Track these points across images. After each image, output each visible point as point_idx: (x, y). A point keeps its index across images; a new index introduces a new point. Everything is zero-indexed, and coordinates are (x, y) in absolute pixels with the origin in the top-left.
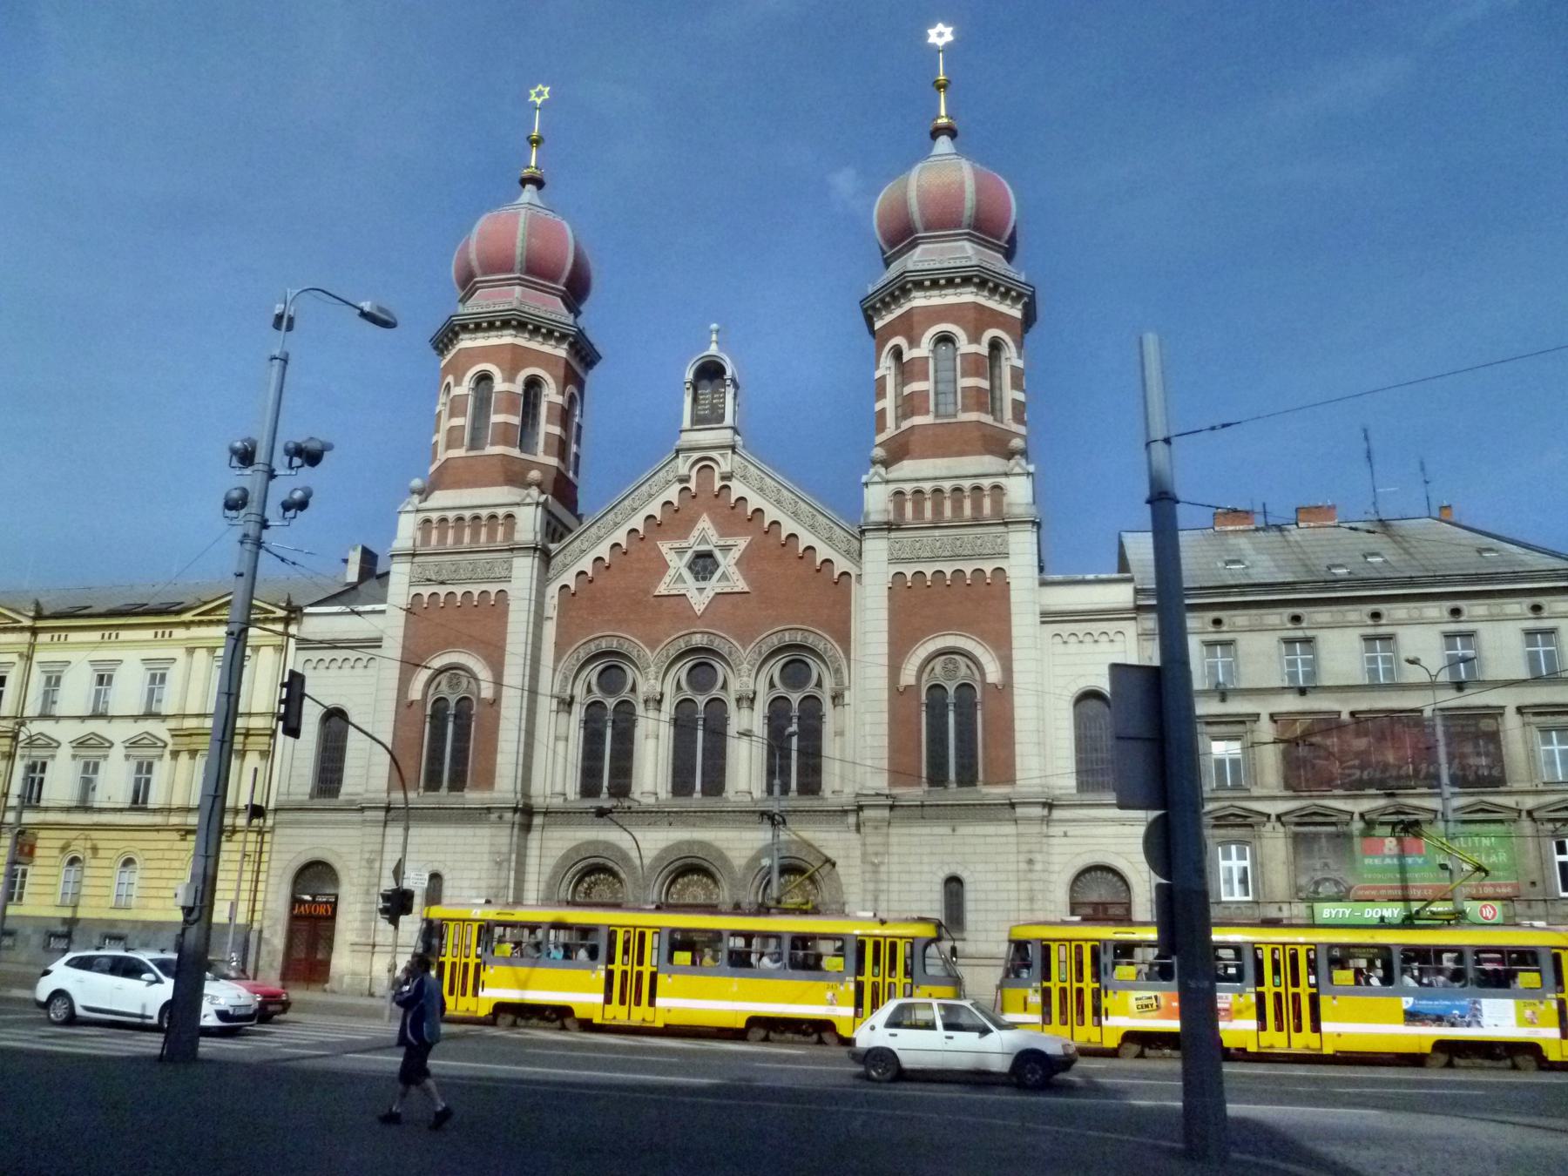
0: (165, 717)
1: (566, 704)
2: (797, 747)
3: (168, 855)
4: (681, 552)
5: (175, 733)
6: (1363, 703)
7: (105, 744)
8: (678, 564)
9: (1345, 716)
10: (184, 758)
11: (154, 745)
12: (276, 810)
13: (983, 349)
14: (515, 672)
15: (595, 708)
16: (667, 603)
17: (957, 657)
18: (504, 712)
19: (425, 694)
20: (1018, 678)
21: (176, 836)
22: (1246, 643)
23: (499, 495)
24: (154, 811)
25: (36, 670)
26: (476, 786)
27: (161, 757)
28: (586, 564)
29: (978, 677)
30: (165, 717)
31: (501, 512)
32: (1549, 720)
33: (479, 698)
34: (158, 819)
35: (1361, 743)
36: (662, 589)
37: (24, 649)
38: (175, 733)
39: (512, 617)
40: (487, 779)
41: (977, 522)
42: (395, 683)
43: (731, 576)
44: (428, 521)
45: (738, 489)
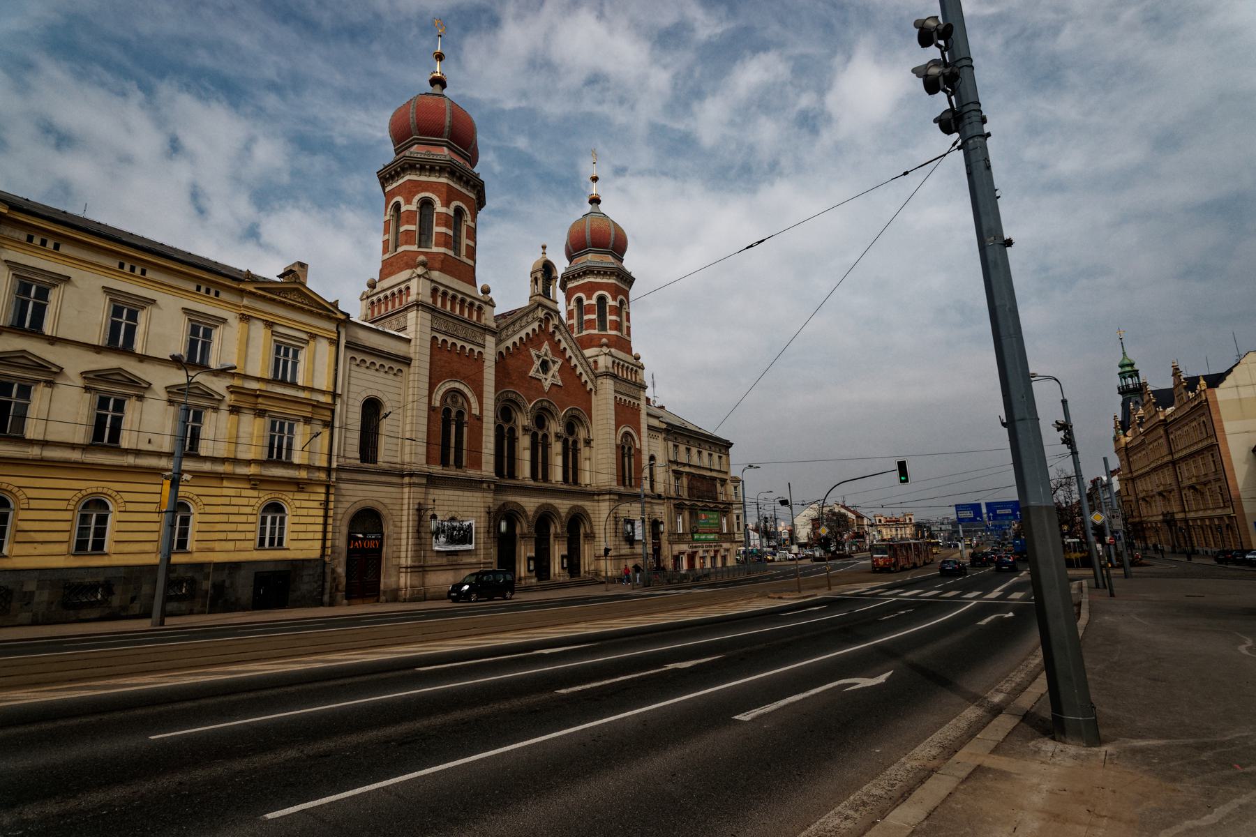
3: (235, 500)
4: (538, 357)
5: (233, 390)
8: (537, 363)
12: (339, 469)
34: (220, 468)
36: (532, 373)
40: (477, 464)
45: (558, 337)
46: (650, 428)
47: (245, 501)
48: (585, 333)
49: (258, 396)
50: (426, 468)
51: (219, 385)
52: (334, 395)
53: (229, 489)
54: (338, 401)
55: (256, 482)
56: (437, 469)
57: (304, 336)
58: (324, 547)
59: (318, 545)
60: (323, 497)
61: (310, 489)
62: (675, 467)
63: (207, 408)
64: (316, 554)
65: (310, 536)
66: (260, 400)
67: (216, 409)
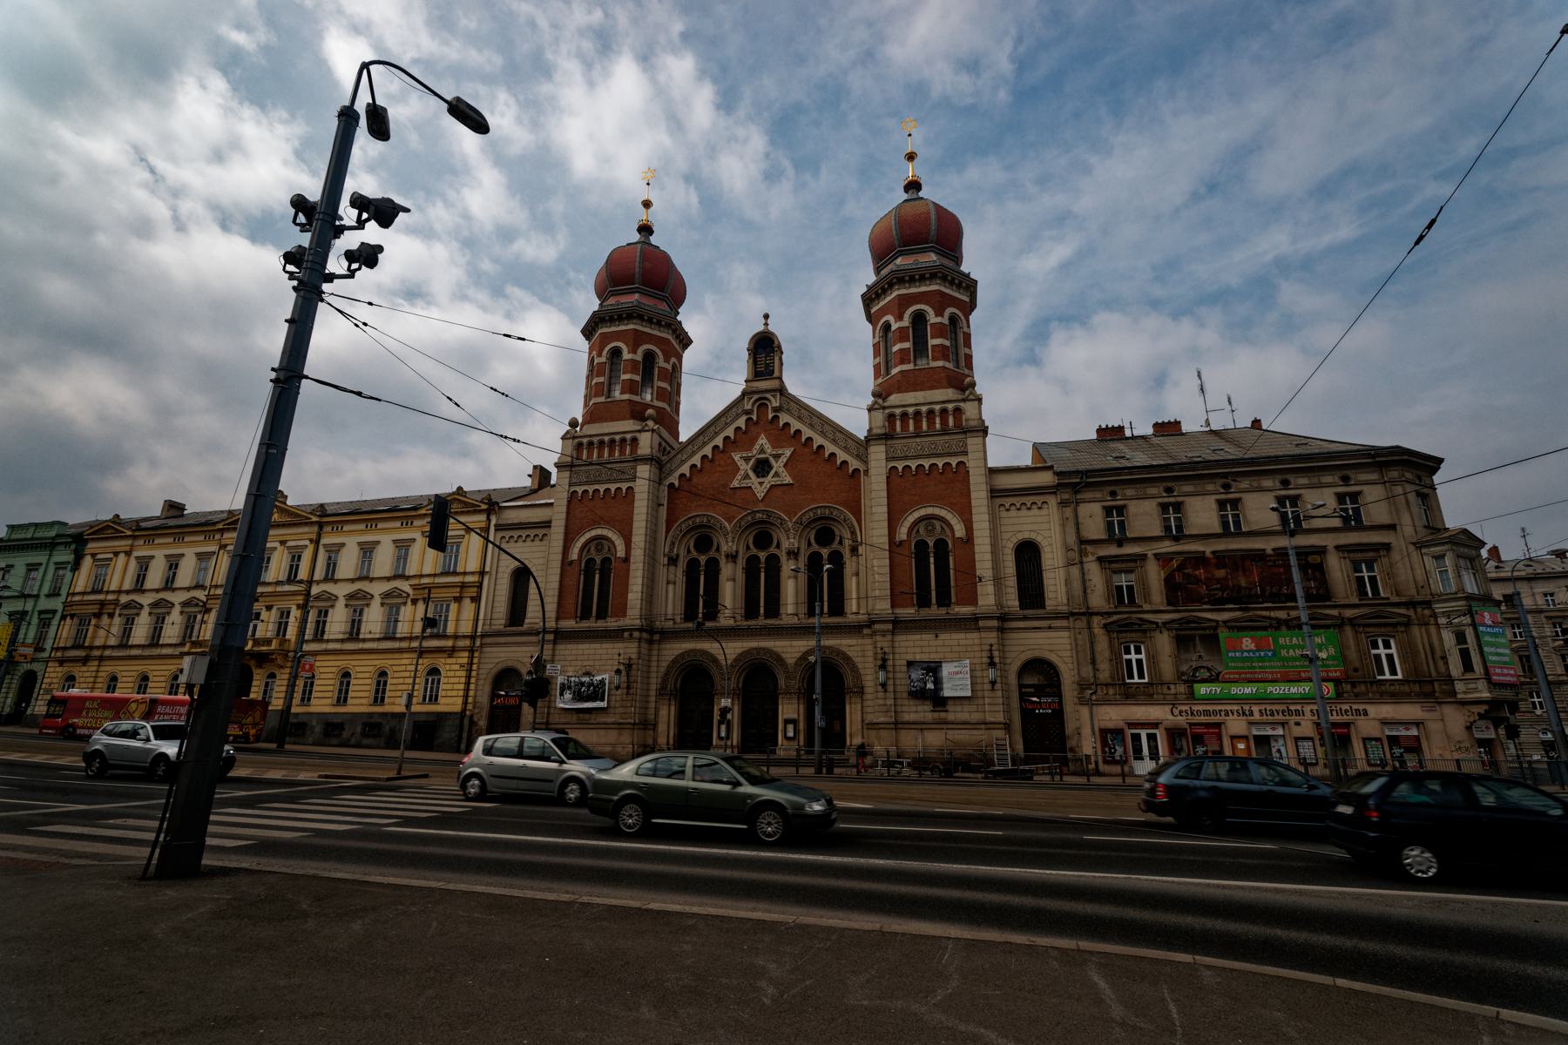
0: (408, 578)
1: (673, 561)
2: (826, 586)
4: (747, 460)
6: (1221, 545)
7: (366, 597)
8: (745, 467)
9: (1208, 554)
11: (400, 596)
12: (482, 636)
13: (945, 321)
14: (639, 538)
15: (692, 566)
18: (632, 567)
22: (1134, 508)
23: (628, 425)
24: (401, 639)
25: (321, 550)
30: (408, 578)
32: (1359, 556)
34: (404, 644)
35: (1221, 573)
36: (735, 484)
37: (314, 537)
39: (637, 504)
40: (622, 611)
41: (945, 431)
42: (560, 549)
43: (781, 473)
44: (580, 445)
45: (784, 418)
51: (405, 586)
55: (422, 652)
58: (465, 703)
59: (460, 701)
60: (465, 661)
62: (1113, 550)
64: (458, 708)
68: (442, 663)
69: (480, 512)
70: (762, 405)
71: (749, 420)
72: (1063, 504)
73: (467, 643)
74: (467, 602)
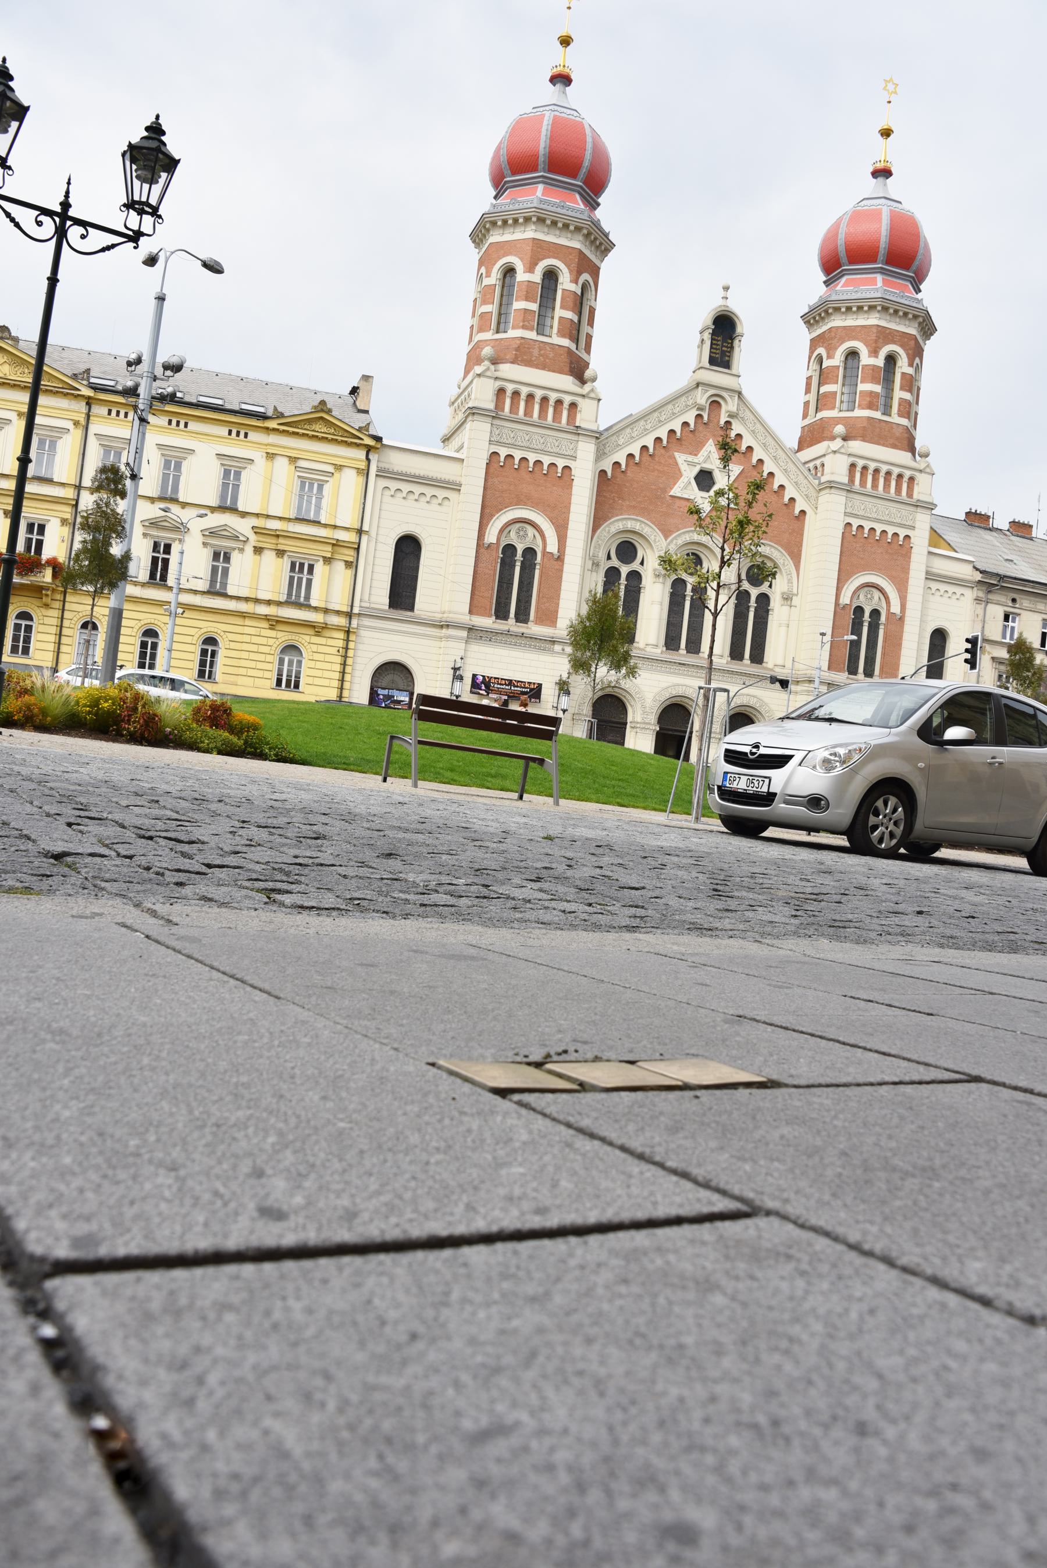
0: (244, 515)
1: (596, 565)
3: (255, 639)
4: (692, 464)
5: (257, 531)
8: (689, 473)
10: (269, 556)
11: (235, 538)
16: (678, 503)
17: (874, 590)
19: (498, 539)
20: (908, 613)
21: (265, 625)
26: (539, 621)
27: (241, 550)
28: (621, 457)
29: (884, 605)
30: (244, 515)
31: (567, 399)
33: (544, 552)
34: (243, 607)
36: (676, 491)
37: (82, 419)
38: (257, 531)
39: (575, 490)
40: (549, 617)
45: (737, 428)
46: (931, 576)
47: (264, 641)
48: (820, 415)
49: (278, 536)
50: (466, 619)
51: (244, 527)
52: (360, 532)
53: (250, 627)
54: (364, 538)
55: (274, 623)
56: (487, 622)
57: (330, 469)
60: (341, 643)
61: (327, 633)
63: (234, 549)
65: (326, 682)
66: (281, 540)
67: (241, 550)
68: (305, 640)
69: (358, 445)
70: (715, 405)
71: (699, 416)
72: (978, 600)
73: (342, 621)
74: (340, 566)
